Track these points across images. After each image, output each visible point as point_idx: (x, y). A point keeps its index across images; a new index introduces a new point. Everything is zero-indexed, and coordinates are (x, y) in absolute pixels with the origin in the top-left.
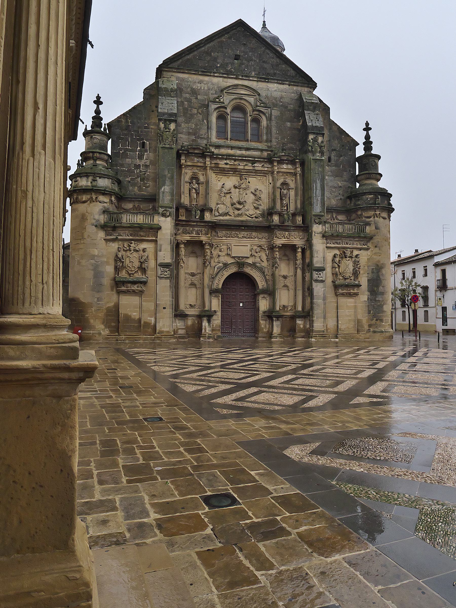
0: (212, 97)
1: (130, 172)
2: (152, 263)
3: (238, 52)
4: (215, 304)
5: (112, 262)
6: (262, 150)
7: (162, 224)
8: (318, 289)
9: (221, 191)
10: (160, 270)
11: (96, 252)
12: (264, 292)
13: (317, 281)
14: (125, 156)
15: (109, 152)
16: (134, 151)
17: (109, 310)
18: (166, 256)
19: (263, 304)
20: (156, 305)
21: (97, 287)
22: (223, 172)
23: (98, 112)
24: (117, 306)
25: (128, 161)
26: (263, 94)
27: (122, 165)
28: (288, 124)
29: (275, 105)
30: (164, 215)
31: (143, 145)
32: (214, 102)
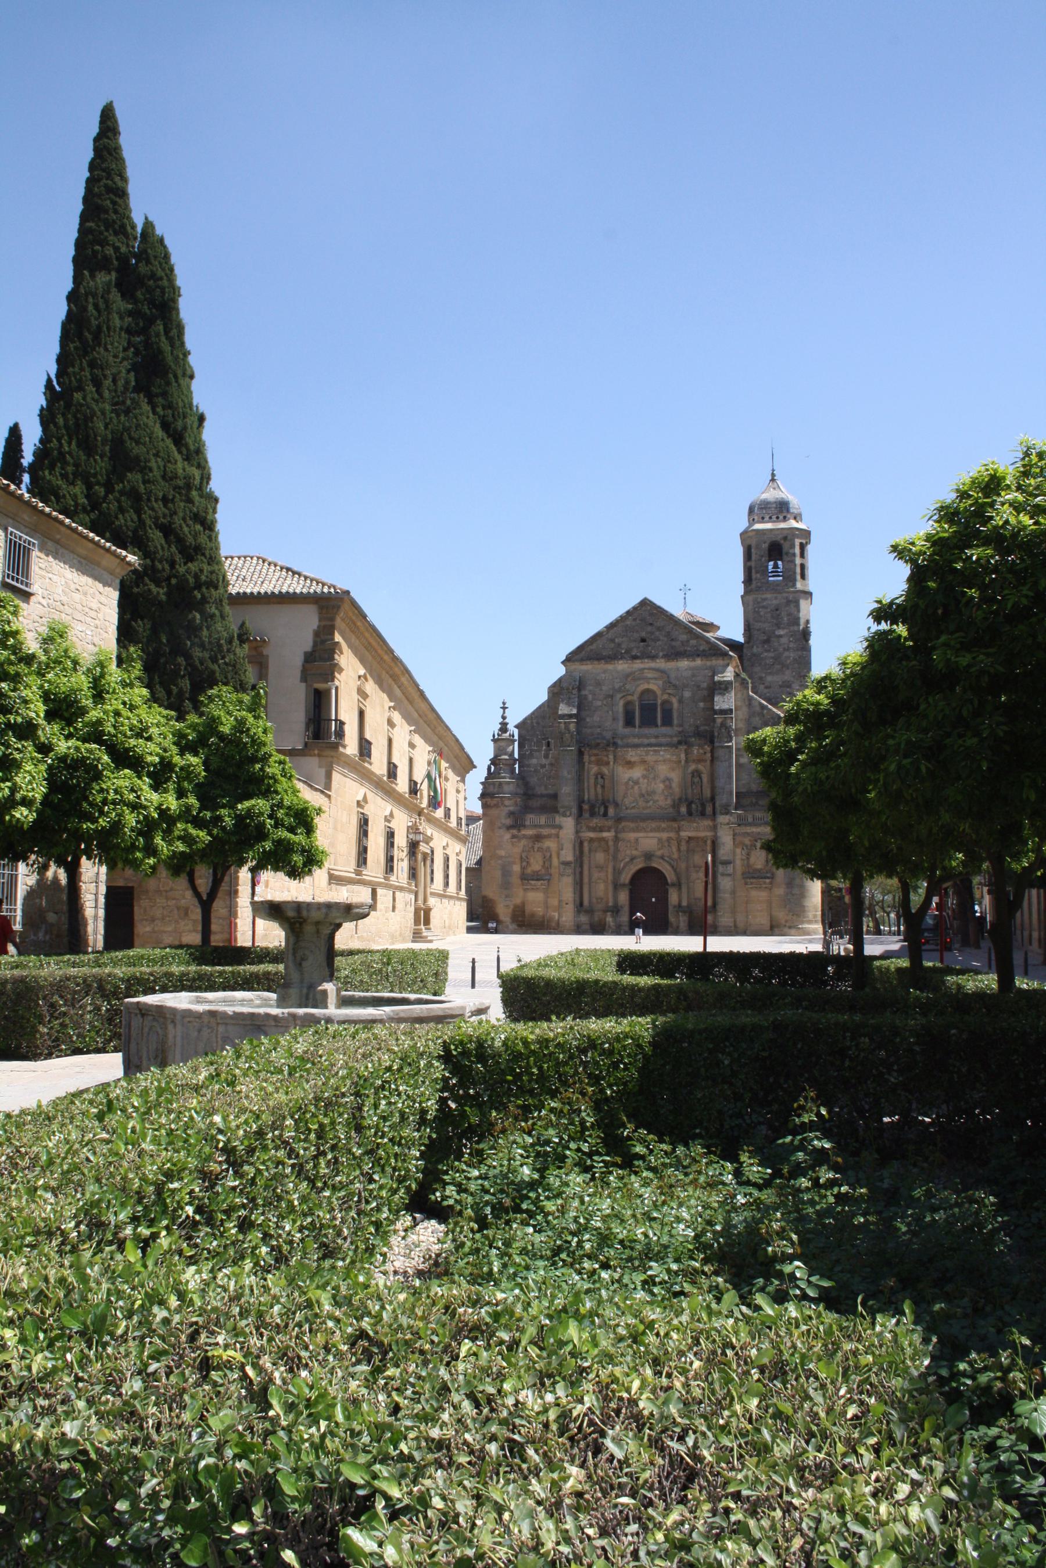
0: (617, 686)
1: (536, 771)
2: (555, 861)
3: (643, 634)
4: (624, 897)
5: (518, 861)
6: (671, 737)
8: (725, 883)
9: (627, 783)
11: (502, 853)
12: (673, 885)
13: (723, 875)
14: (531, 756)
15: (516, 756)
16: (539, 751)
17: (516, 907)
18: (568, 855)
19: (673, 897)
20: (560, 901)
21: (506, 885)
22: (630, 764)
23: (504, 718)
24: (523, 904)
25: (534, 761)
26: (673, 675)
27: (529, 766)
28: (702, 705)
29: (685, 686)
30: (565, 815)
31: (548, 744)
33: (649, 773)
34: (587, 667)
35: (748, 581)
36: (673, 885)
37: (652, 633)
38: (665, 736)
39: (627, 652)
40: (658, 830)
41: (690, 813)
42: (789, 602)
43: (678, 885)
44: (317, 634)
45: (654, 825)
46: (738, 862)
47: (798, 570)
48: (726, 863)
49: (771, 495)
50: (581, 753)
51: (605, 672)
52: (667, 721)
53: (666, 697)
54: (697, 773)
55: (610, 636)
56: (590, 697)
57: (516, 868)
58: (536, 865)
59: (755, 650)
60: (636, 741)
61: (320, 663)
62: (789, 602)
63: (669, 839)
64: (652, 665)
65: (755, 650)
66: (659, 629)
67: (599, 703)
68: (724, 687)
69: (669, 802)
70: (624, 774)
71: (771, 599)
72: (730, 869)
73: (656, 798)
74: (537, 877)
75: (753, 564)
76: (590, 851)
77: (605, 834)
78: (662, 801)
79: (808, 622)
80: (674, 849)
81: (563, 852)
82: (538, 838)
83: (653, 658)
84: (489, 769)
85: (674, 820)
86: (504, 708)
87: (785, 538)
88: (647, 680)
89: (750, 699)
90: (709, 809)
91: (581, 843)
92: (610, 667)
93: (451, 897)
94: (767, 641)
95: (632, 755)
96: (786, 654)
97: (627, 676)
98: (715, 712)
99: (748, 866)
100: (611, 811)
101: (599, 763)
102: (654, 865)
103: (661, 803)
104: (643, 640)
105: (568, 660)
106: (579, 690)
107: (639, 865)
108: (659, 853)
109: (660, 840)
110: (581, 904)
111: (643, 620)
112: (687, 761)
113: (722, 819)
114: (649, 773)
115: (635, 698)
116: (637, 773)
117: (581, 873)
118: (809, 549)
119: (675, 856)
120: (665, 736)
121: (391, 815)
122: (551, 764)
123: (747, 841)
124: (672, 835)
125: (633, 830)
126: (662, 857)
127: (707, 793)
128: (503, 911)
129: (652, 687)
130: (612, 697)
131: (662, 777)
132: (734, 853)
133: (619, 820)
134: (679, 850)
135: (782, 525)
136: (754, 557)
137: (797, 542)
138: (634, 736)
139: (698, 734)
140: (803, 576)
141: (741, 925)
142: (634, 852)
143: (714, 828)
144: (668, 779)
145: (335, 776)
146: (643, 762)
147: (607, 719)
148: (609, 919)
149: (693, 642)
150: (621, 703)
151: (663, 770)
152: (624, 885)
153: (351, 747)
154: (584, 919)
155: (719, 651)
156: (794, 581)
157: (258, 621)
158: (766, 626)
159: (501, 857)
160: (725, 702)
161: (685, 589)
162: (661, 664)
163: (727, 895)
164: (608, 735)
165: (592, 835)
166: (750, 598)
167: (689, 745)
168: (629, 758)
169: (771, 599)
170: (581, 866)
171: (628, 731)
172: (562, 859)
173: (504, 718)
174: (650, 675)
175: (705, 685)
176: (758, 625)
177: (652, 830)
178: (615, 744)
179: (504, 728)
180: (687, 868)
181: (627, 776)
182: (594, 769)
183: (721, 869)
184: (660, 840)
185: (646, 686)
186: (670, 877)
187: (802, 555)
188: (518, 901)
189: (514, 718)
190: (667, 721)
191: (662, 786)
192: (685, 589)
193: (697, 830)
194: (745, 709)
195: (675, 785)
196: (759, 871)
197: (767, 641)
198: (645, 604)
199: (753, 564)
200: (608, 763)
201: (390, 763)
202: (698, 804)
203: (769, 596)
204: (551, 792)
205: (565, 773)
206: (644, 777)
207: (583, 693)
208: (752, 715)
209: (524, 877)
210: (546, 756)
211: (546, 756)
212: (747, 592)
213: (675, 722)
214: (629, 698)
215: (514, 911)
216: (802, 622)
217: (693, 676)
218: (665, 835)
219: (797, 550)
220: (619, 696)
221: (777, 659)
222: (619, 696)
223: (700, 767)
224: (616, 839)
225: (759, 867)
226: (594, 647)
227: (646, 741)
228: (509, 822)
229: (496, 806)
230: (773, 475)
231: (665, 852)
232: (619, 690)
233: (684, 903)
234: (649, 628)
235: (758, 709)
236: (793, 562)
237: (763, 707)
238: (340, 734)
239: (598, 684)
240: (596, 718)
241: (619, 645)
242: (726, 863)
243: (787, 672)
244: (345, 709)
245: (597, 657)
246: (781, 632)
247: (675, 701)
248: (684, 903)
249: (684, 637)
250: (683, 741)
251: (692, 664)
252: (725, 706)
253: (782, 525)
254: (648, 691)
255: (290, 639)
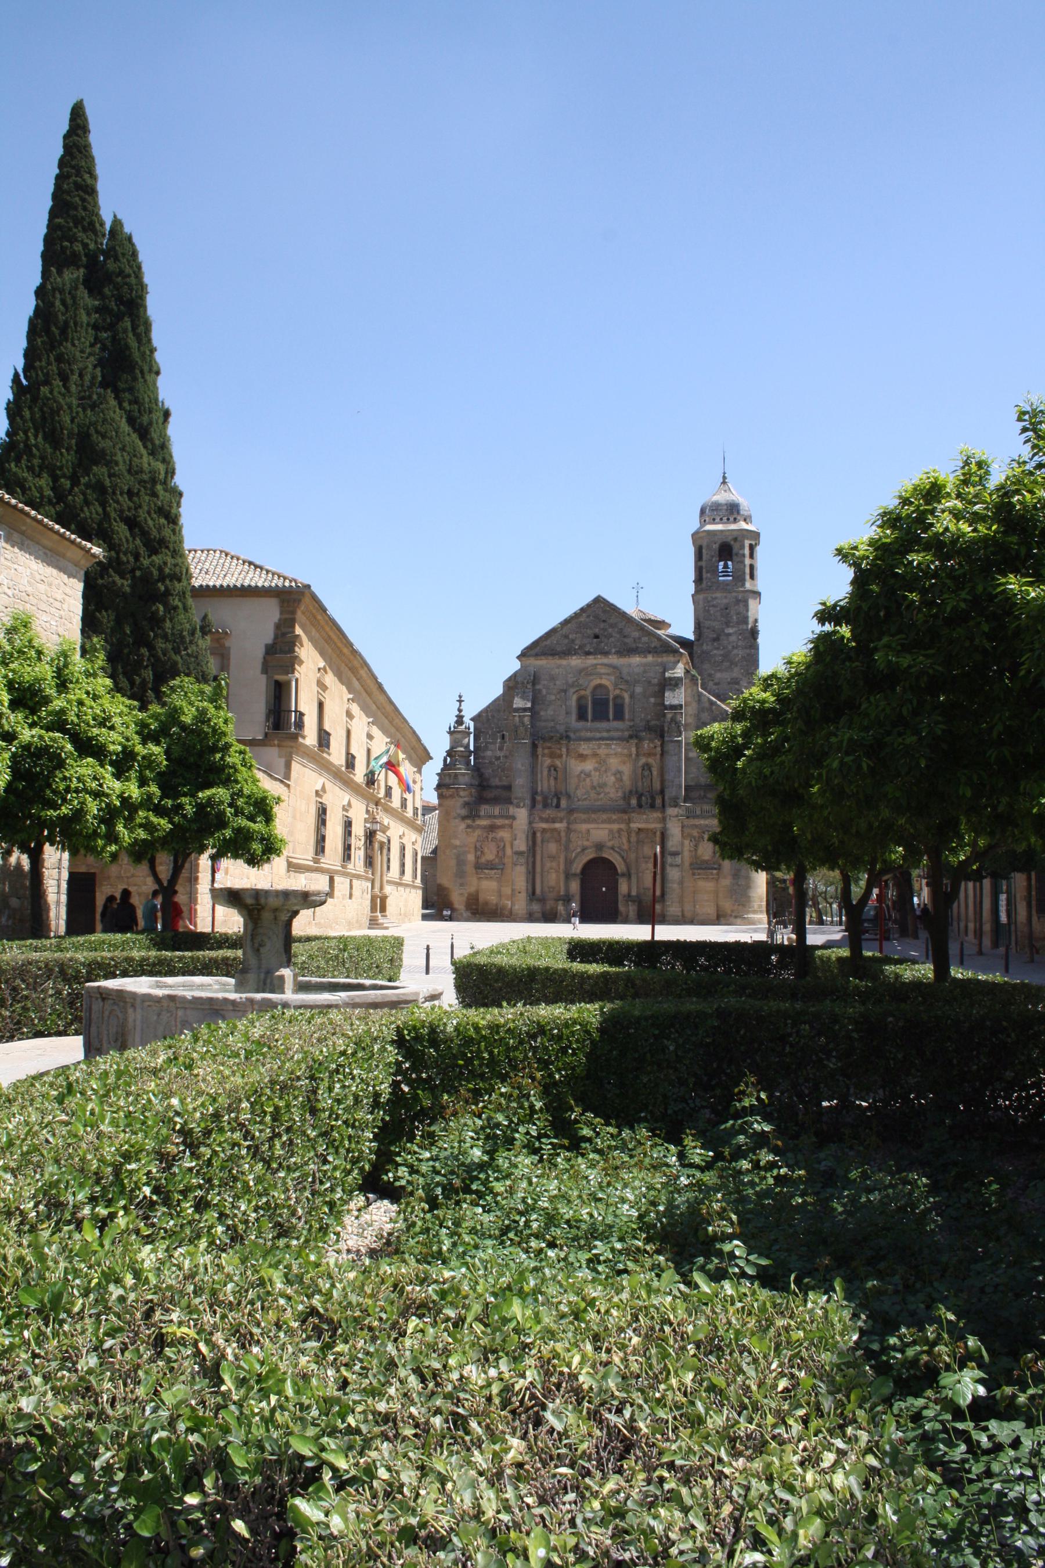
0: (570, 681)
1: (491, 763)
2: (509, 851)
3: (597, 631)
4: (575, 886)
5: (472, 850)
6: (622, 731)
7: (517, 815)
8: (673, 874)
9: (579, 776)
10: (515, 857)
11: (457, 842)
12: (623, 875)
13: (671, 865)
14: (486, 748)
15: (472, 748)
16: (494, 743)
17: (470, 894)
18: (521, 845)
19: (623, 887)
21: (460, 874)
22: (582, 757)
23: (460, 711)
24: (477, 892)
25: (489, 753)
26: (625, 671)
27: (484, 758)
28: (652, 700)
29: (637, 682)
30: (518, 806)
31: (503, 737)
32: (572, 686)
33: (602, 765)
34: (542, 662)
35: (699, 580)
36: (623, 875)
37: (605, 630)
38: (617, 730)
39: (581, 647)
40: (610, 821)
41: (640, 806)
42: (738, 601)
43: (628, 875)
44: (278, 626)
45: (605, 816)
46: (686, 854)
47: (747, 570)
48: (675, 854)
49: (722, 497)
50: (534, 746)
51: (559, 667)
52: (619, 715)
53: (618, 692)
54: (647, 767)
55: (565, 631)
56: (544, 692)
57: (471, 857)
58: (490, 855)
59: (705, 647)
60: (589, 734)
61: (280, 655)
62: (738, 601)
63: (620, 830)
64: (605, 661)
65: (705, 647)
66: (612, 626)
67: (553, 697)
68: (675, 683)
69: (620, 794)
70: (577, 767)
71: (720, 598)
72: (678, 860)
73: (607, 790)
74: (491, 866)
75: (703, 564)
76: (542, 841)
77: (557, 825)
78: (613, 794)
79: (756, 621)
80: (625, 841)
81: (516, 843)
82: (492, 828)
83: (605, 654)
84: (445, 760)
85: (625, 812)
86: (460, 701)
87: (735, 539)
88: (600, 675)
89: (700, 695)
90: (658, 801)
91: (534, 834)
92: (564, 662)
93: (407, 885)
94: (717, 639)
95: (584, 748)
96: (735, 651)
97: (581, 671)
98: (666, 707)
99: (696, 857)
100: (564, 803)
101: (552, 755)
102: (605, 855)
103: (612, 795)
104: (597, 637)
105: (523, 655)
106: (534, 684)
107: (590, 855)
108: (610, 844)
109: (611, 831)
110: (534, 893)
111: (596, 617)
112: (637, 755)
113: (671, 811)
114: (602, 765)
115: (588, 692)
116: (589, 766)
117: (534, 863)
118: (759, 550)
119: (625, 847)
120: (617, 730)
121: (349, 804)
122: (506, 757)
123: (695, 833)
124: (623, 826)
125: (585, 821)
126: (613, 848)
127: (657, 786)
128: (458, 899)
129: (604, 682)
130: (565, 691)
131: (614, 770)
132: (682, 844)
133: (571, 811)
134: (629, 841)
135: (733, 527)
136: (704, 557)
137: (747, 543)
138: (587, 730)
139: (649, 728)
140: (752, 577)
141: (688, 914)
142: (586, 843)
143: (664, 820)
144: (619, 772)
145: (295, 766)
146: (595, 755)
147: (560, 713)
148: (561, 908)
149: (645, 639)
150: (575, 697)
151: (614, 762)
152: (575, 875)
153: (310, 737)
154: (536, 907)
155: (669, 648)
156: (743, 581)
157: (221, 614)
158: (716, 625)
159: (456, 847)
160: (675, 697)
161: (638, 588)
162: (613, 660)
163: (675, 886)
164: (561, 729)
165: (544, 825)
166: (701, 597)
167: (640, 739)
168: (581, 751)
169: (720, 598)
170: (534, 856)
171: (581, 724)
172: (516, 849)
173: (460, 711)
174: (602, 671)
175: (656, 681)
176: (707, 623)
177: (603, 822)
178: (568, 737)
179: (460, 720)
180: (637, 859)
181: (579, 769)
182: (548, 761)
183: (669, 859)
184: (611, 831)
185: (598, 681)
186: (621, 867)
187: (752, 556)
188: (472, 889)
189: (470, 712)
190: (619, 715)
191: (613, 778)
192: (638, 588)
193: (647, 821)
194: (694, 705)
195: (625, 778)
196: (706, 862)
197: (717, 639)
198: (599, 602)
199: (703, 564)
200: (560, 756)
201: (348, 753)
202: (647, 797)
203: (718, 595)
204: (505, 783)
205: (519, 766)
206: (596, 769)
207: (538, 687)
208: (701, 710)
209: (479, 867)
210: (501, 749)
211: (501, 749)
212: (697, 591)
213: (627, 716)
214: (582, 693)
215: (468, 899)
216: (751, 620)
217: (645, 672)
218: (615, 827)
219: (747, 551)
220: (572, 690)
221: (726, 656)
222: (572, 690)
223: (650, 760)
224: (568, 830)
225: (706, 858)
226: (548, 642)
227: (598, 735)
228: (464, 812)
229: (452, 796)
230: (724, 478)
231: (615, 843)
232: (572, 686)
233: (634, 893)
234: (602, 625)
235: (707, 705)
236: (743, 562)
237: (712, 703)
238: (300, 725)
239: (553, 678)
240: (550, 712)
241: (573, 641)
242: (675, 854)
243: (736, 670)
244: (305, 701)
245: (552, 653)
246: (730, 630)
247: (626, 696)
248: (634, 893)
249: (636, 634)
250: (634, 736)
251: (644, 660)
252: (675, 702)
253: (733, 527)
254: (600, 686)
255: (251, 632)
